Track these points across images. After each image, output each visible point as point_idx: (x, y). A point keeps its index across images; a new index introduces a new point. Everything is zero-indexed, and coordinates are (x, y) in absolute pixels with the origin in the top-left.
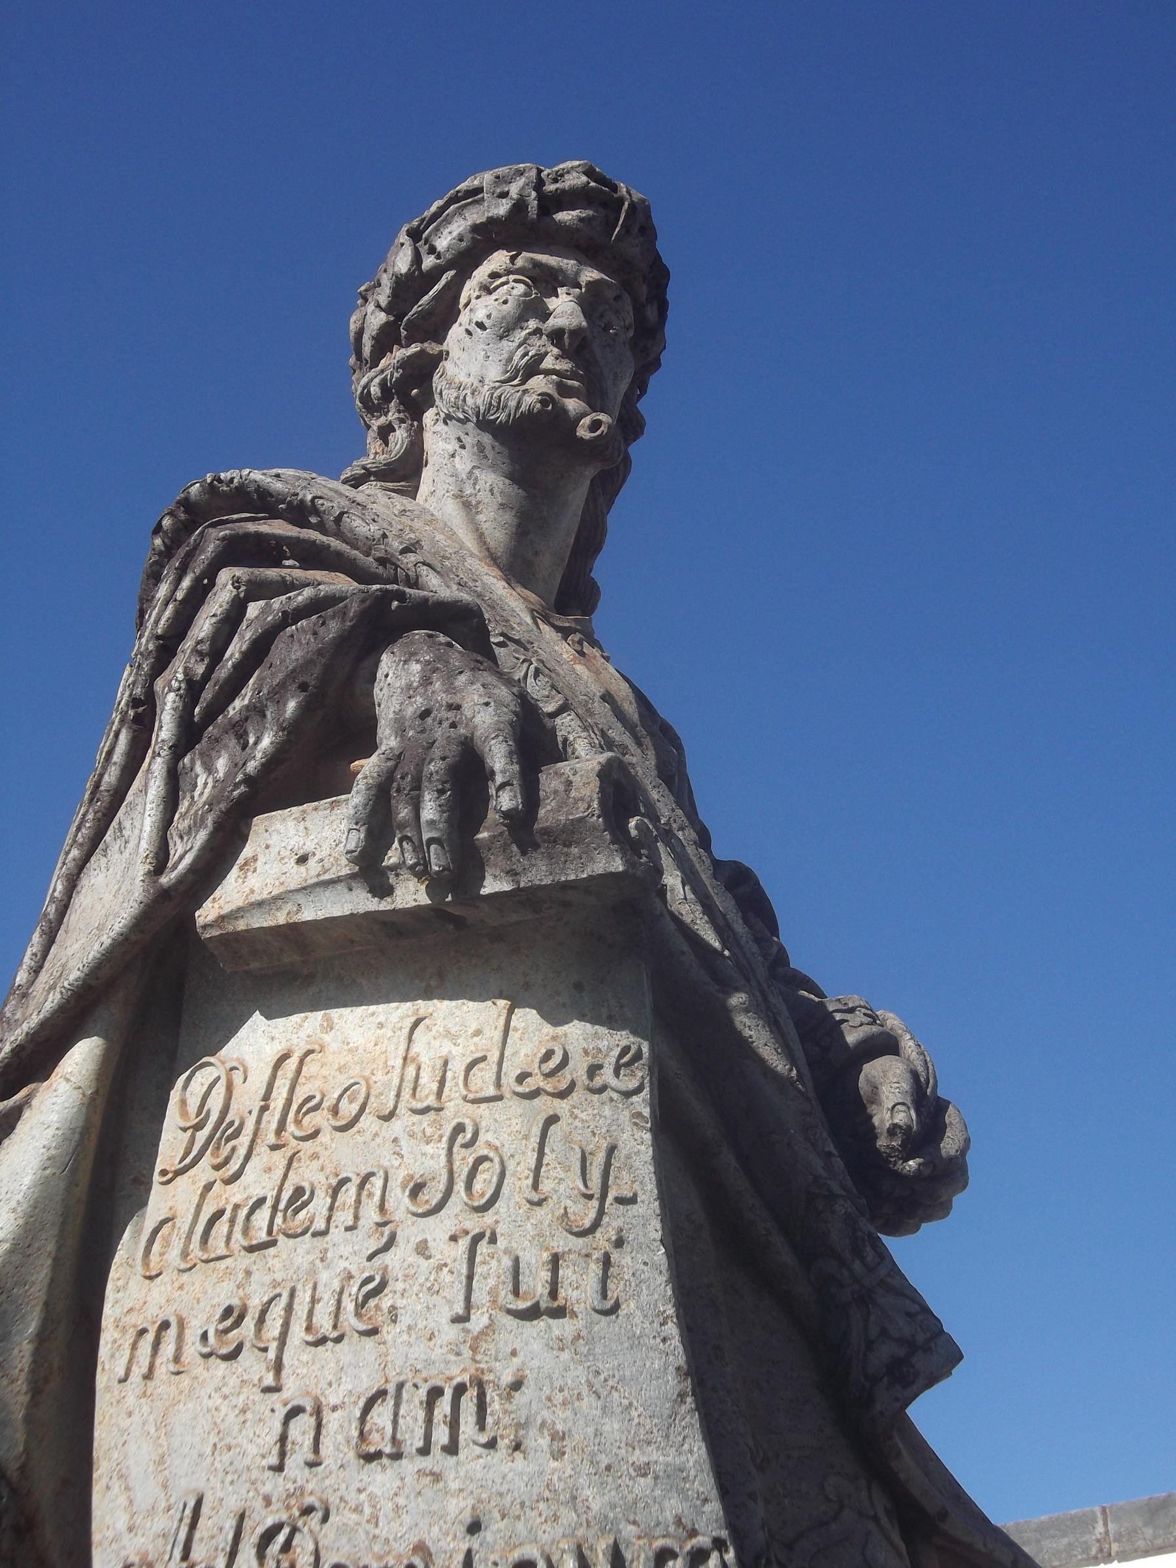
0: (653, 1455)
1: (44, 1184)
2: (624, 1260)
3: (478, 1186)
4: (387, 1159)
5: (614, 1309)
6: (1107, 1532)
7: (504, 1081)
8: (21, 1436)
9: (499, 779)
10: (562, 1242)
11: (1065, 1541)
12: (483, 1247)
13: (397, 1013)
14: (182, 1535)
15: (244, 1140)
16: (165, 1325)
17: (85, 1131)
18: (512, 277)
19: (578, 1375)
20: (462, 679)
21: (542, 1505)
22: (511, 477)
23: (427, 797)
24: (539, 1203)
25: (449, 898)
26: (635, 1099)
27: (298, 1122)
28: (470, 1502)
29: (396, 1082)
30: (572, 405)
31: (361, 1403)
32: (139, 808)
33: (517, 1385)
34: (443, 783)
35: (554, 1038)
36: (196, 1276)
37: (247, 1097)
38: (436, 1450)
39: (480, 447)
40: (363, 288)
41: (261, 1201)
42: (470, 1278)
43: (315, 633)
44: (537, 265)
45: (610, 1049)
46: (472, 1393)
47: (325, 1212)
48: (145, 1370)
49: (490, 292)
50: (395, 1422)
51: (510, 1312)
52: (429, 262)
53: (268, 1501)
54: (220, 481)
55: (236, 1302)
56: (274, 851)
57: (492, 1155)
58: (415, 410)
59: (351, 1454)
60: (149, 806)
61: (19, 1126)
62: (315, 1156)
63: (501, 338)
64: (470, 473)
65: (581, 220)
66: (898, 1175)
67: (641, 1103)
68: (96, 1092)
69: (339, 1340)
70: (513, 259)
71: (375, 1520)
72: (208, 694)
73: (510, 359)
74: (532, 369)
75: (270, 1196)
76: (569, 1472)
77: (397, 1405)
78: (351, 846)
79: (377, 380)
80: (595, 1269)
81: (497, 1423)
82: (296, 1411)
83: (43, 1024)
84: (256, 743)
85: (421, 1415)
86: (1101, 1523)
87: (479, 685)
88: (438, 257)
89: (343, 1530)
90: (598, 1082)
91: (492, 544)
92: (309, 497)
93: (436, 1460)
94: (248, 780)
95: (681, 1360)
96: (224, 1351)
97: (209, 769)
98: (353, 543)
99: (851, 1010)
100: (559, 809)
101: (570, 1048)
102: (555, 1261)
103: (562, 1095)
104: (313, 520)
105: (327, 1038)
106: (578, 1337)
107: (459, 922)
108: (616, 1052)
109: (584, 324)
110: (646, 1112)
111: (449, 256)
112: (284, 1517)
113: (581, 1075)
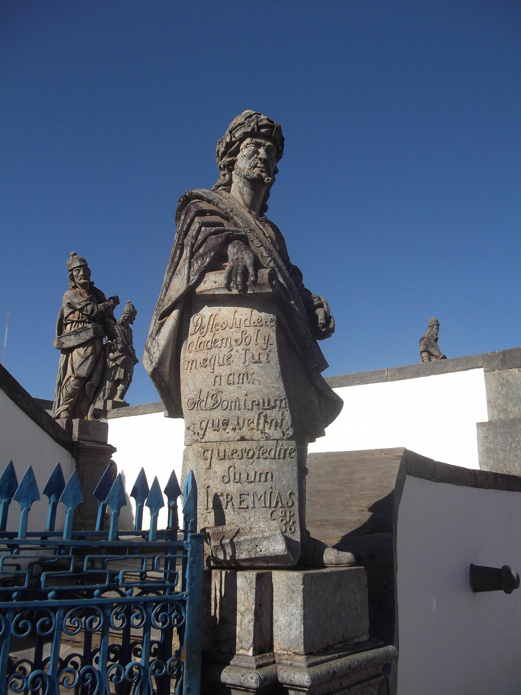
0: (275, 385)
1: (170, 336)
2: (271, 354)
3: (247, 341)
4: (231, 335)
5: (269, 362)
6: (388, 375)
7: (251, 323)
8: (168, 377)
9: (251, 275)
10: (261, 351)
11: (377, 376)
12: (248, 351)
13: (232, 309)
14: (199, 395)
15: (205, 330)
16: (193, 361)
17: (176, 326)
18: (251, 145)
19: (263, 372)
20: (244, 253)
22: (251, 189)
23: (238, 277)
24: (257, 345)
25: (242, 293)
26: (273, 327)
27: (215, 327)
28: (246, 391)
29: (232, 322)
30: (264, 175)
31: (228, 376)
32: (184, 268)
33: (253, 374)
34: (241, 274)
35: (260, 316)
36: (198, 353)
37: (205, 322)
38: (240, 383)
39: (245, 182)
40: (219, 141)
41: (209, 341)
42: (245, 356)
43: (216, 239)
44: (256, 142)
45: (269, 318)
46: (246, 375)
47: (220, 344)
48: (190, 368)
49: (247, 148)
50: (233, 379)
51: (252, 362)
52: (233, 139)
53: (213, 390)
54: (192, 192)
55: (206, 358)
56: (210, 280)
58: (231, 171)
59: (226, 383)
60: (186, 269)
61: (164, 325)
62: (218, 334)
63: (249, 159)
64: (242, 187)
65: (266, 131)
66: (322, 331)
67: (274, 328)
68: (178, 320)
69: (224, 365)
70: (252, 140)
72: (195, 247)
73: (251, 164)
74: (255, 166)
75: (211, 340)
76: (261, 387)
77: (234, 376)
78: (225, 283)
79: (222, 164)
80: (266, 356)
81: (250, 379)
82: (217, 376)
83: (168, 308)
84: (206, 260)
85: (238, 378)
86: (386, 372)
87: (247, 254)
88: (236, 138)
89: (226, 395)
90: (267, 324)
91: (247, 202)
92: (211, 199)
93: (240, 385)
94: (205, 267)
95: (280, 370)
96: (204, 366)
97: (197, 263)
98: (220, 209)
99: (315, 298)
100: (261, 280)
101: (262, 318)
102: (259, 354)
103: (261, 326)
104: (212, 203)
105: (219, 312)
106: (263, 366)
107: (243, 296)
108: (270, 319)
109: (266, 157)
110: (275, 329)
111: (238, 139)
113: (264, 323)
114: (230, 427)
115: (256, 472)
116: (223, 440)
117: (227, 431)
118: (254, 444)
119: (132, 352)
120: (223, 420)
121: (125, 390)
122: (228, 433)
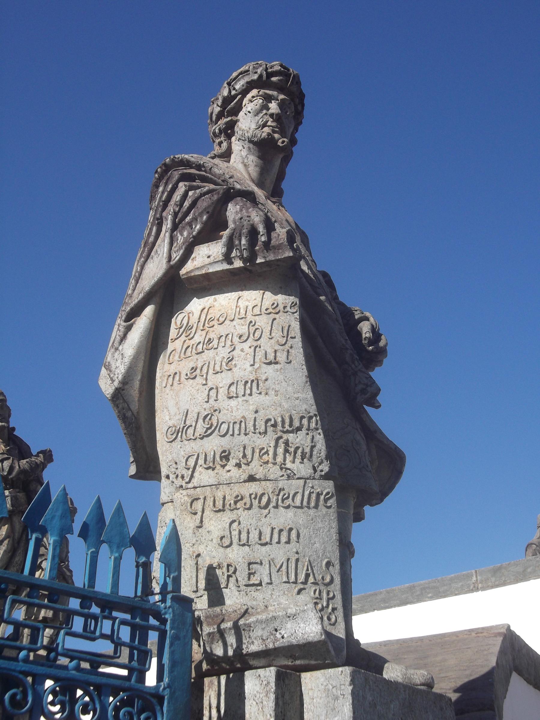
0: (299, 395)
1: (141, 342)
2: (292, 351)
3: (256, 335)
4: (232, 330)
5: (290, 362)
6: (477, 580)
7: (262, 311)
8: (137, 404)
9: (261, 234)
10: (277, 347)
11: (460, 584)
12: (258, 349)
13: (233, 295)
14: (184, 419)
15: (193, 330)
16: (176, 373)
17: (150, 329)
18: (258, 97)
19: (281, 377)
20: (251, 209)
21: (273, 407)
22: (259, 157)
23: (243, 238)
24: (271, 339)
25: (248, 264)
26: (295, 314)
27: (208, 324)
28: (255, 406)
29: (234, 312)
30: (276, 136)
31: (228, 386)
32: (163, 246)
33: (266, 380)
34: (247, 235)
35: (275, 300)
36: (183, 362)
37: (194, 320)
38: (247, 395)
39: (249, 148)
40: (212, 99)
41: (200, 343)
42: (254, 356)
43: (210, 199)
44: (266, 94)
45: (289, 302)
46: (256, 382)
47: (217, 343)
48: (171, 384)
49: (252, 102)
50: (237, 389)
51: (265, 363)
52: (233, 92)
53: (205, 409)
54: (175, 158)
55: (194, 366)
56: (201, 255)
57: (259, 328)
58: (229, 137)
59: (226, 397)
60: (165, 245)
61: (132, 329)
62: (213, 331)
63: (255, 116)
64: (246, 156)
65: (279, 80)
66: (368, 351)
67: (297, 315)
68: (153, 319)
69: (222, 372)
70: (259, 92)
71: (232, 412)
72: (180, 215)
73: (258, 122)
74: (265, 125)
76: (279, 399)
77: (237, 386)
78: (223, 252)
79: (218, 128)
80: (285, 353)
81: (262, 389)
82: (211, 389)
83: (139, 302)
84: (195, 227)
85: (243, 387)
86: (475, 576)
87: (255, 211)
88: (236, 91)
89: (225, 414)
90: (286, 310)
91: (253, 177)
92: (202, 163)
93: (247, 397)
94: (193, 237)
95: (307, 374)
96: (192, 377)
97: (182, 235)
98: (215, 175)
99: (356, 311)
100: (277, 240)
101: (279, 303)
102: (276, 351)
103: (277, 313)
104: (203, 169)
105: (215, 303)
106: (281, 369)
107: (250, 271)
108: (291, 303)
109: (280, 112)
110: (298, 317)
111: (239, 91)
112: (209, 412)
113: (282, 309)
114: (233, 462)
115: (273, 529)
116: (221, 482)
117: (227, 468)
118: (269, 486)
119: (68, 573)
120: (221, 451)
121: (54, 638)
122: (229, 471)
